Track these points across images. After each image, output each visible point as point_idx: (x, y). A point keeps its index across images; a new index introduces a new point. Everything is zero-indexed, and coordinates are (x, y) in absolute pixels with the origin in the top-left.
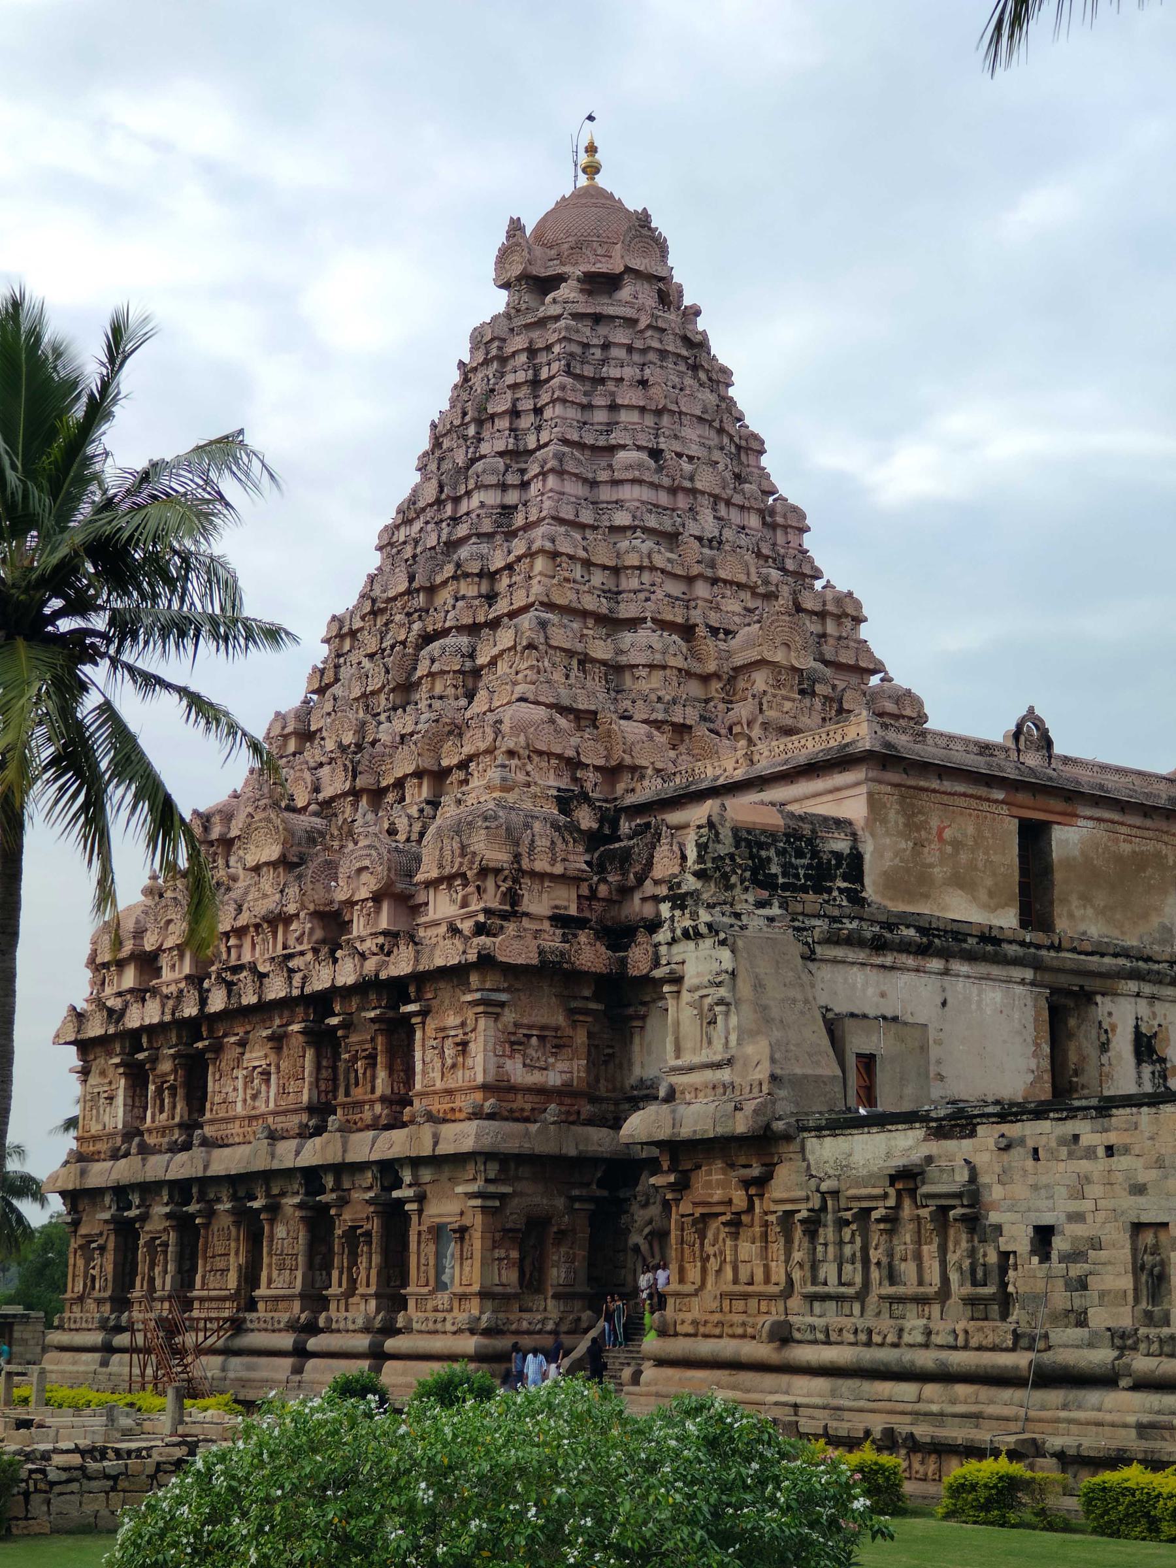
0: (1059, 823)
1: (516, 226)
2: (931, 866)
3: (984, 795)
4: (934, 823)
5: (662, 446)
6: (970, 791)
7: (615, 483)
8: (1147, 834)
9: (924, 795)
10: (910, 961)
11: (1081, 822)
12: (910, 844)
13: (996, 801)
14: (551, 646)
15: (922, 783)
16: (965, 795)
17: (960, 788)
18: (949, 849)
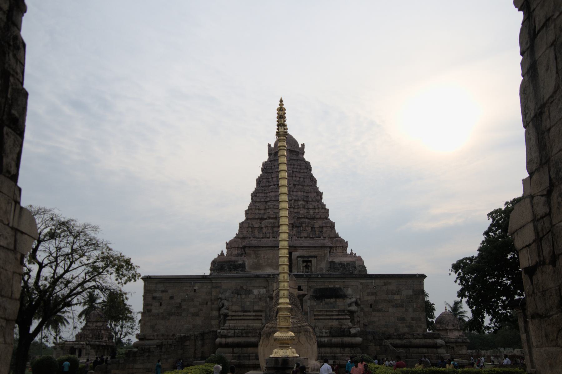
0: (294, 252)
1: (269, 145)
2: (262, 263)
3: (273, 249)
4: (262, 256)
6: (270, 249)
7: (269, 192)
8: (316, 251)
9: (260, 251)
11: (299, 251)
12: (257, 260)
13: (277, 250)
14: (244, 227)
15: (258, 249)
16: (269, 250)
17: (268, 249)
18: (266, 260)
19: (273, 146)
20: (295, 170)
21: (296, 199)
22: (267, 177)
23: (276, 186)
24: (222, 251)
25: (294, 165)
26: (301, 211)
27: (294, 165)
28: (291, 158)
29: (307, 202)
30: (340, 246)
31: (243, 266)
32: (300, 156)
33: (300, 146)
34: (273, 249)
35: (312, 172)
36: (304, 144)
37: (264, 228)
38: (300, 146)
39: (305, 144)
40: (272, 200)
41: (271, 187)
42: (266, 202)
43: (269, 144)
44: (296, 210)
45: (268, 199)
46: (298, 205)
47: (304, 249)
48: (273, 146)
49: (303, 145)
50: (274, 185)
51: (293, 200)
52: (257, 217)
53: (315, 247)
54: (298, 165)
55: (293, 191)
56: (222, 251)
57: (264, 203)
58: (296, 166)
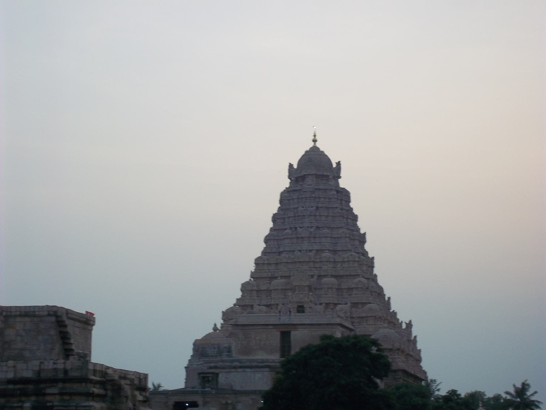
1: (291, 166)
5: (297, 226)
10: (233, 370)
19: (295, 166)
20: (320, 205)
21: (319, 249)
22: (283, 217)
23: (293, 229)
24: (215, 325)
25: (319, 198)
26: (324, 266)
27: (319, 198)
28: (317, 187)
29: (335, 252)
30: (372, 316)
31: (229, 350)
32: (332, 183)
33: (334, 165)
34: (266, 327)
35: (352, 205)
36: (339, 162)
37: (273, 291)
38: (334, 165)
39: (341, 163)
40: (286, 251)
41: (286, 231)
42: (280, 253)
43: (290, 163)
44: (317, 265)
45: (281, 250)
46: (320, 258)
47: (306, 327)
48: (295, 166)
49: (339, 164)
50: (291, 228)
51: (314, 250)
52: (265, 275)
53: (320, 325)
54: (325, 198)
55: (314, 237)
56: (215, 325)
57: (277, 254)
58: (322, 199)
